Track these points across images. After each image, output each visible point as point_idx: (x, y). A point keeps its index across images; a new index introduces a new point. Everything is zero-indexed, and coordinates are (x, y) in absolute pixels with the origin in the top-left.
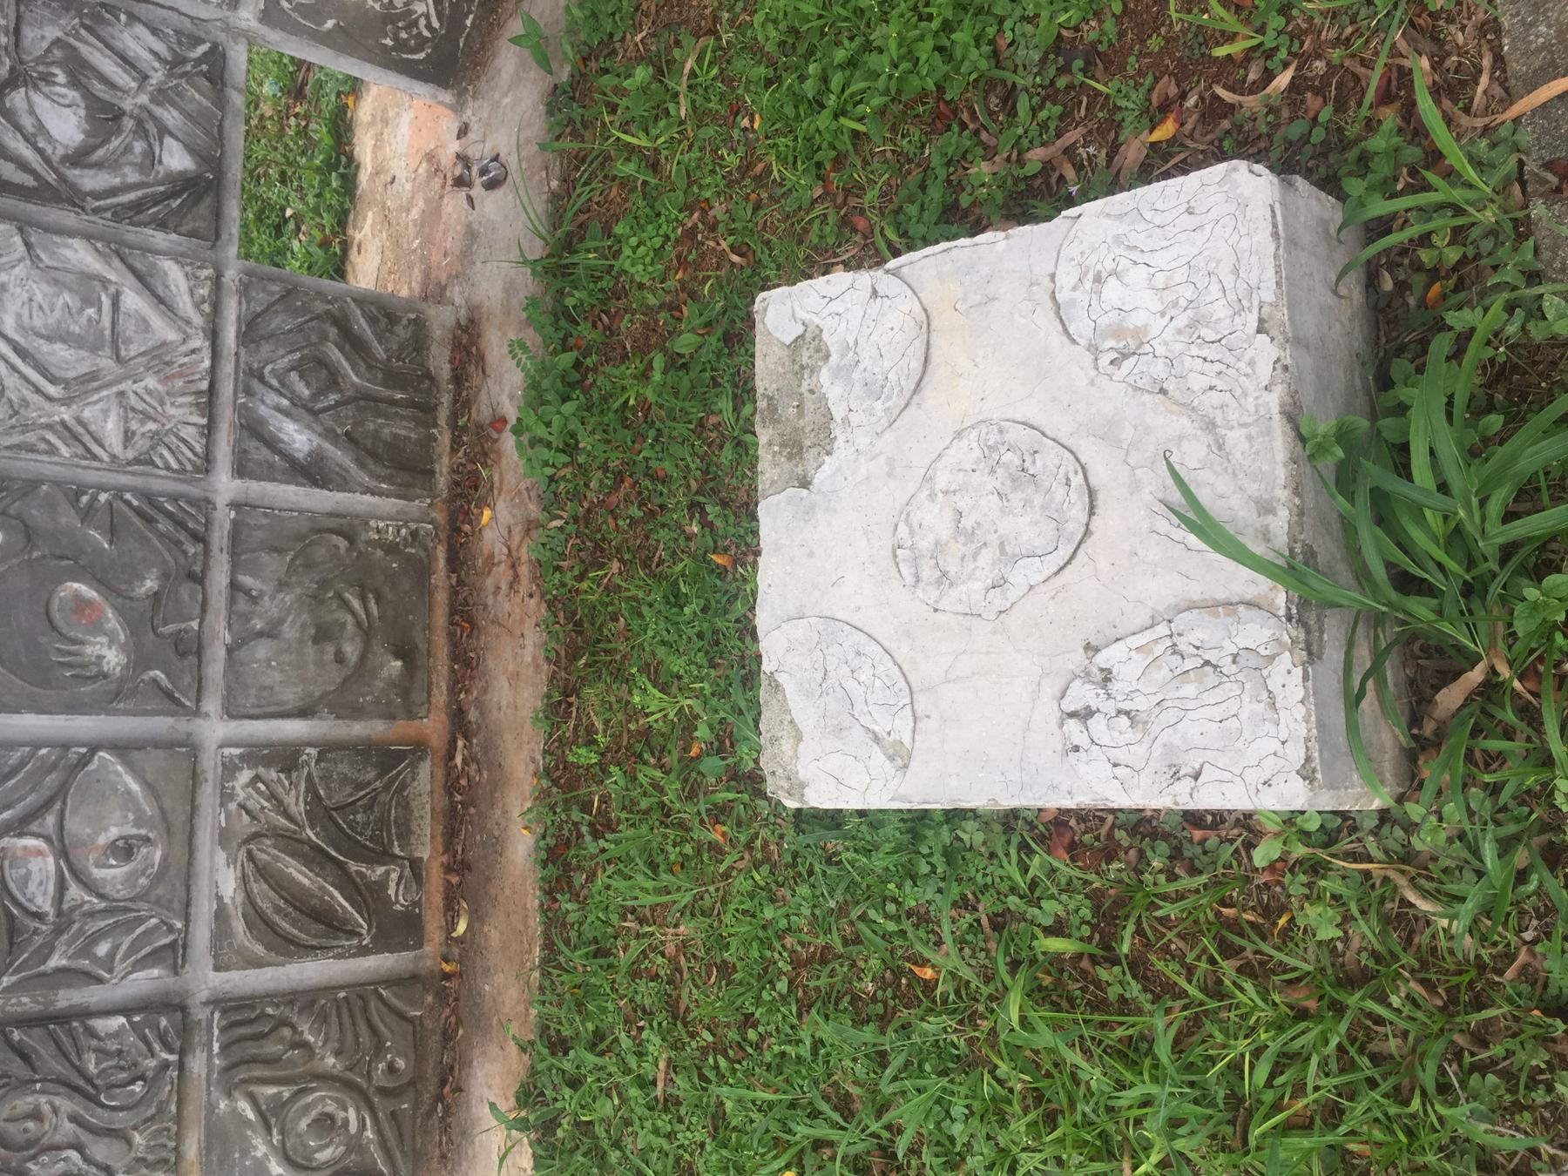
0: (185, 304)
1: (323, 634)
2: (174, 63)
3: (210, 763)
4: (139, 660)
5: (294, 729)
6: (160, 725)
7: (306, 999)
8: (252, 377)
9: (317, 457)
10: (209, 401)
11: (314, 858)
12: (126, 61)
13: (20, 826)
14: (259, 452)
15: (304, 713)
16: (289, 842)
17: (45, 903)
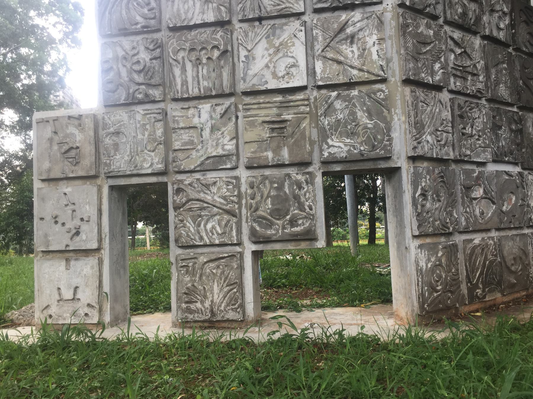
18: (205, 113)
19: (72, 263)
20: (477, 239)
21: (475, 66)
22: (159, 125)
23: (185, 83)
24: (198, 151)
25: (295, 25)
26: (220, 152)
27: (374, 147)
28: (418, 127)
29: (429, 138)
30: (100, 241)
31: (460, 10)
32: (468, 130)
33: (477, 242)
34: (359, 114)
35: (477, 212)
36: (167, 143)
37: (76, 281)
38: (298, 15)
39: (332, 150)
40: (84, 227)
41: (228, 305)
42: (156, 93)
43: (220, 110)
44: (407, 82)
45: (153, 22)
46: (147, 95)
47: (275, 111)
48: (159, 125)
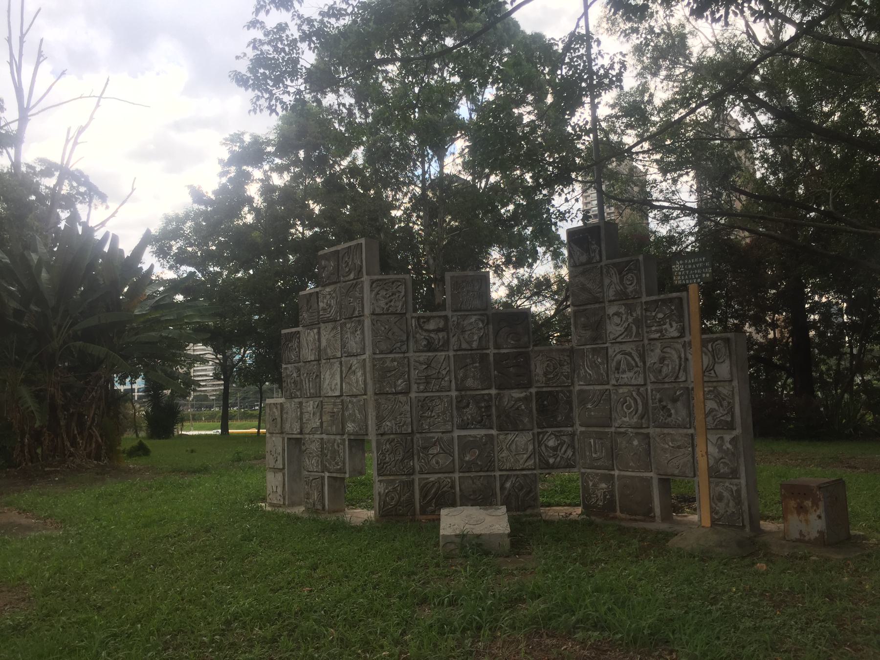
0: (527, 464)
3: (451, 475)
4: (467, 462)
5: (458, 489)
6: (457, 467)
7: (413, 494)
8: (518, 476)
10: (511, 470)
11: (436, 493)
12: (565, 452)
13: (441, 448)
14: (504, 479)
15: (460, 490)
16: (438, 489)
17: (430, 452)
20: (433, 478)
28: (380, 419)
29: (388, 423)
30: (284, 465)
31: (425, 343)
36: (301, 419)
44: (376, 394)
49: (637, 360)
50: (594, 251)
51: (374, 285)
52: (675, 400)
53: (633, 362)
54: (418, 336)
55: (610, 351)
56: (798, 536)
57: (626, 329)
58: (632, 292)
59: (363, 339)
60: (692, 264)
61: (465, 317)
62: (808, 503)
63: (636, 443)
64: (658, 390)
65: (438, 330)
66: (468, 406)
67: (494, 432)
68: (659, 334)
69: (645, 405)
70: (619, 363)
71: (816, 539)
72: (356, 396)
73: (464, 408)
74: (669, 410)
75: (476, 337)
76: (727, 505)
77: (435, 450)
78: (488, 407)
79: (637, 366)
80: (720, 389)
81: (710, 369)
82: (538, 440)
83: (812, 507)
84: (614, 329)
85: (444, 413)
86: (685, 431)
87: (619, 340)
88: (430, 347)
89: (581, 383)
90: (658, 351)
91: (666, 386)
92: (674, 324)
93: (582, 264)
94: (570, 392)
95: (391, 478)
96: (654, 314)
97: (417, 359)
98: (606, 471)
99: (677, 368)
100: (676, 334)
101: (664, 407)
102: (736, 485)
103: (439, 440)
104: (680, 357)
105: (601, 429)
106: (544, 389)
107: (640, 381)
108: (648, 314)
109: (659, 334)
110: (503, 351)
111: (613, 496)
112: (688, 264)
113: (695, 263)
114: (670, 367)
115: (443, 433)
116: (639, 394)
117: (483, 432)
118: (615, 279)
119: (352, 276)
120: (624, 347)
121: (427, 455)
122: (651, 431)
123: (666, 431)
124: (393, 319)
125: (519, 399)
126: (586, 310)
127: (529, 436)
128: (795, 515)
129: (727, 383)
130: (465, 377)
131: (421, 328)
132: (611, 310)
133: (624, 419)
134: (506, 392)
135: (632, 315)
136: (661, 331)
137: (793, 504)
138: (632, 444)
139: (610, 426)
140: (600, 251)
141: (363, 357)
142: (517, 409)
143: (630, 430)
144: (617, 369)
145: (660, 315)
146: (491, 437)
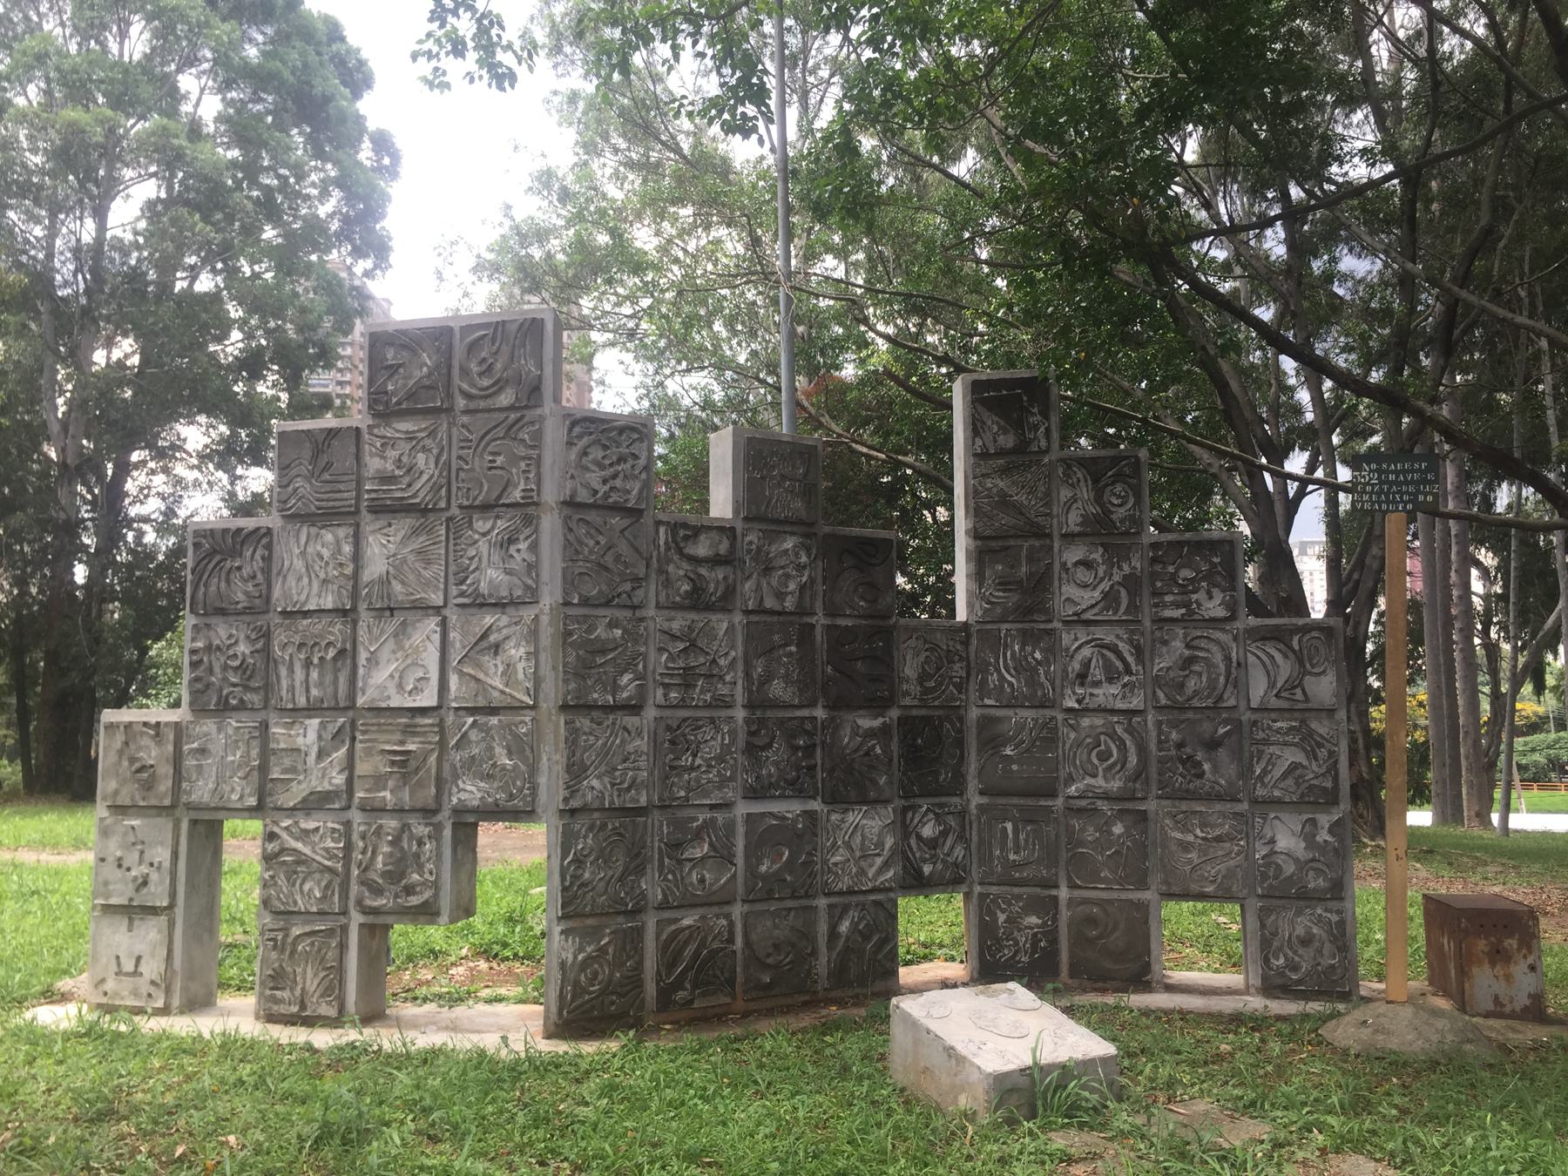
1: (776, 947)
2: (955, 864)
3: (726, 909)
4: (765, 877)
6: (740, 890)
7: (640, 963)
9: (838, 935)
10: (851, 892)
12: (952, 848)
13: (711, 844)
14: (836, 914)
15: (748, 943)
16: (702, 945)
18: (309, 734)
19: (136, 923)
21: (714, 661)
22: (254, 743)
23: (292, 689)
24: (299, 782)
25: (432, 624)
26: (326, 786)
27: (511, 797)
29: (595, 783)
30: (173, 895)
31: (686, 587)
32: (686, 760)
33: (686, 922)
34: (498, 750)
35: (694, 877)
37: (140, 948)
38: (437, 610)
39: (463, 796)
40: (154, 876)
41: (322, 996)
42: (254, 699)
43: (332, 728)
44: (564, 708)
45: (257, 601)
46: (242, 700)
47: (398, 736)
48: (254, 743)
49: (1130, 659)
50: (1036, 428)
51: (577, 430)
52: (1212, 745)
53: (1118, 664)
54: (671, 568)
55: (1066, 639)
56: (1491, 1007)
57: (1106, 595)
58: (1122, 521)
59: (532, 567)
60: (1397, 473)
61: (771, 537)
62: (1512, 943)
63: (1118, 829)
64: (1174, 725)
65: (716, 561)
66: (770, 745)
67: (816, 805)
68: (1183, 611)
69: (1142, 750)
70: (1086, 664)
71: (1526, 1009)
72: (493, 711)
73: (763, 749)
74: (1199, 764)
75: (792, 586)
76: (1320, 951)
77: (700, 851)
78: (809, 750)
79: (1128, 671)
80: (1314, 725)
81: (1294, 684)
82: (904, 829)
83: (1519, 950)
84: (1076, 594)
85: (720, 759)
86: (1228, 807)
87: (1088, 616)
88: (698, 600)
89: (988, 702)
90: (1178, 644)
91: (1190, 715)
92: (1218, 596)
93: (1001, 453)
94: (961, 719)
95: (590, 922)
96: (1171, 569)
97: (666, 626)
98: (1038, 890)
99: (1222, 679)
100: (1221, 613)
101: (1190, 757)
102: (1339, 912)
103: (709, 825)
104: (1228, 658)
105: (1030, 802)
106: (914, 712)
107: (1136, 702)
108: (1158, 568)
109: (1183, 611)
110: (842, 622)
111: (1054, 941)
112: (1388, 472)
113: (1404, 472)
114: (1204, 679)
115: (712, 807)
116: (1130, 730)
117: (791, 808)
118: (1085, 493)
119: (505, 399)
120: (1099, 633)
121: (680, 862)
122: (1151, 806)
123: (1184, 806)
124: (616, 521)
125: (871, 733)
126: (1007, 548)
127: (887, 814)
128: (1487, 967)
129: (1324, 715)
130: (766, 680)
131: (680, 551)
132: (1073, 555)
133: (1088, 780)
134: (849, 716)
135: (1120, 568)
136: (1187, 605)
137: (1482, 945)
138: (1110, 833)
139: (1053, 795)
140: (1048, 430)
141: (528, 613)
142: (867, 754)
143: (1099, 803)
144: (1082, 677)
145: (1187, 573)
146: (810, 816)
